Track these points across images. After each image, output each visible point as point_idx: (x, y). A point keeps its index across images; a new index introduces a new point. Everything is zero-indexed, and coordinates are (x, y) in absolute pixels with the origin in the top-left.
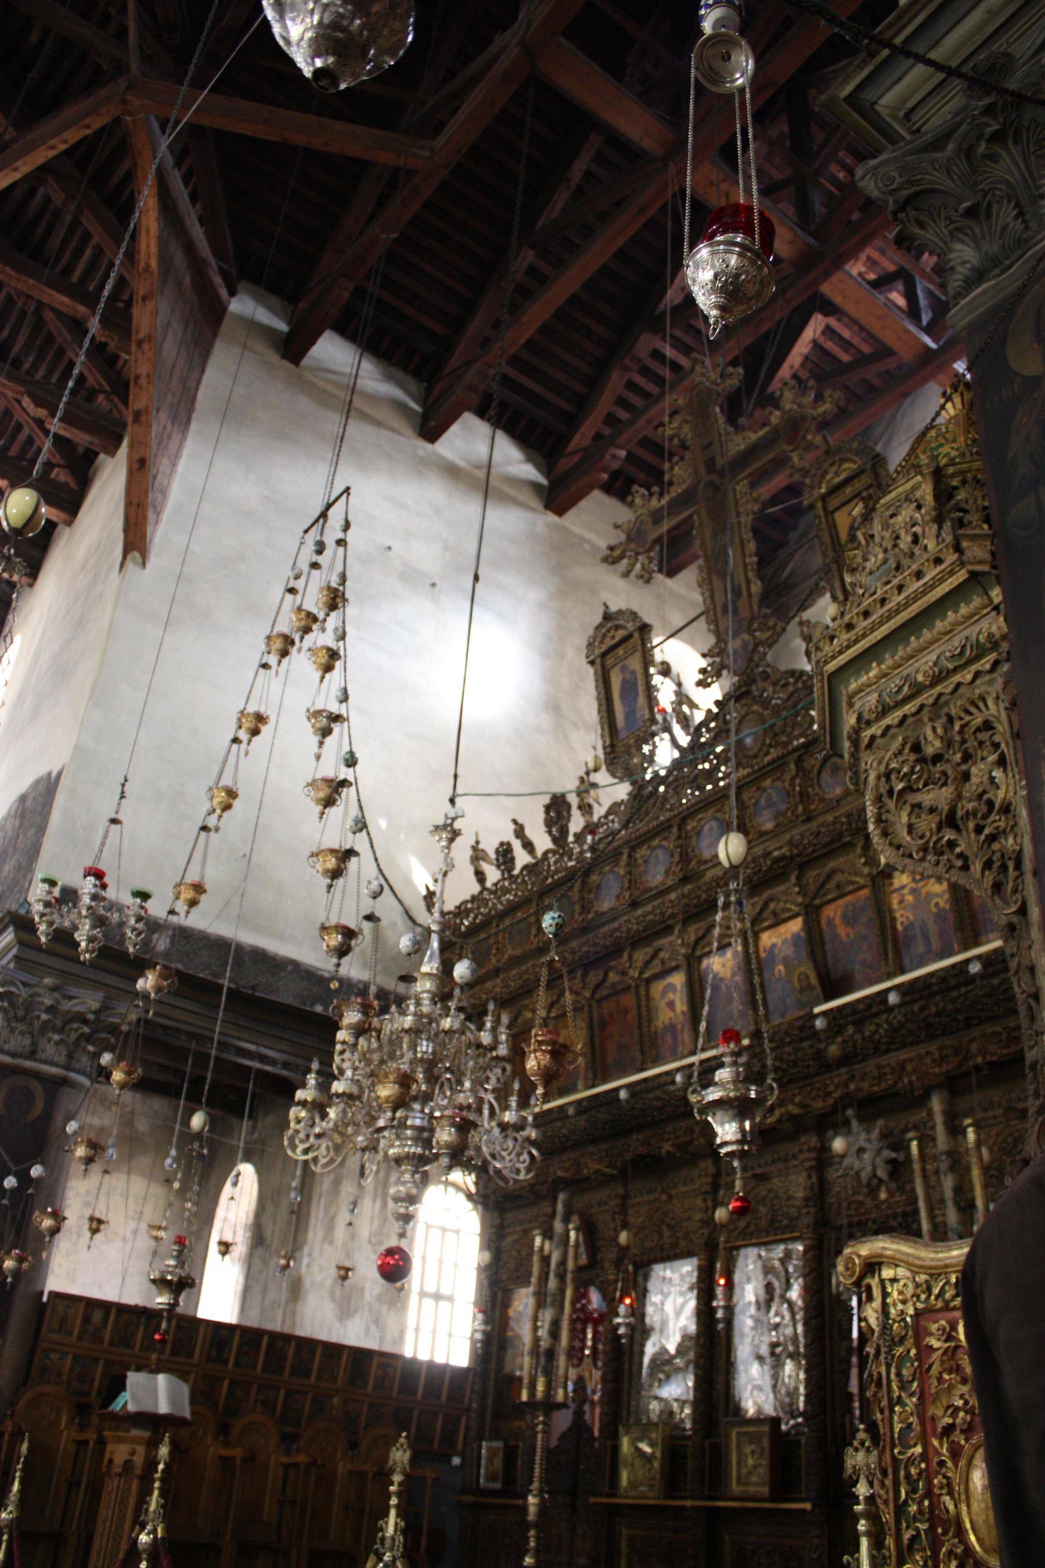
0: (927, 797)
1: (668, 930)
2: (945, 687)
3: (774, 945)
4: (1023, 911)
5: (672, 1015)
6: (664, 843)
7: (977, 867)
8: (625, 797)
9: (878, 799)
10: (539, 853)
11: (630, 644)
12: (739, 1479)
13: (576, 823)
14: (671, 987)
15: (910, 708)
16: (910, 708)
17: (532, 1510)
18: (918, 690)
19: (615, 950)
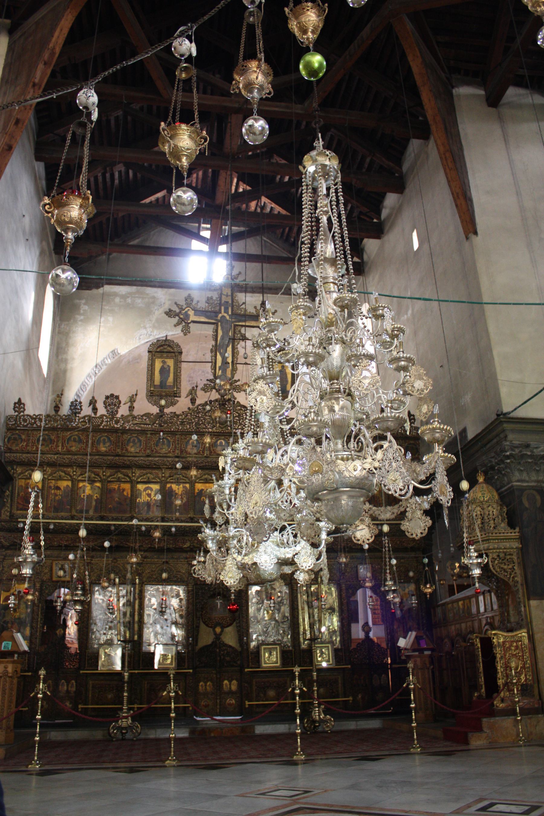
0: (502, 566)
1: (159, 468)
2: (508, 550)
3: (202, 490)
4: (518, 589)
5: (149, 499)
6: (169, 438)
7: (511, 579)
8: (155, 413)
9: (492, 562)
10: (99, 414)
11: (170, 355)
13: (123, 411)
14: (151, 489)
15: (501, 550)
16: (501, 550)
17: (126, 677)
18: (505, 548)
19: (129, 467)
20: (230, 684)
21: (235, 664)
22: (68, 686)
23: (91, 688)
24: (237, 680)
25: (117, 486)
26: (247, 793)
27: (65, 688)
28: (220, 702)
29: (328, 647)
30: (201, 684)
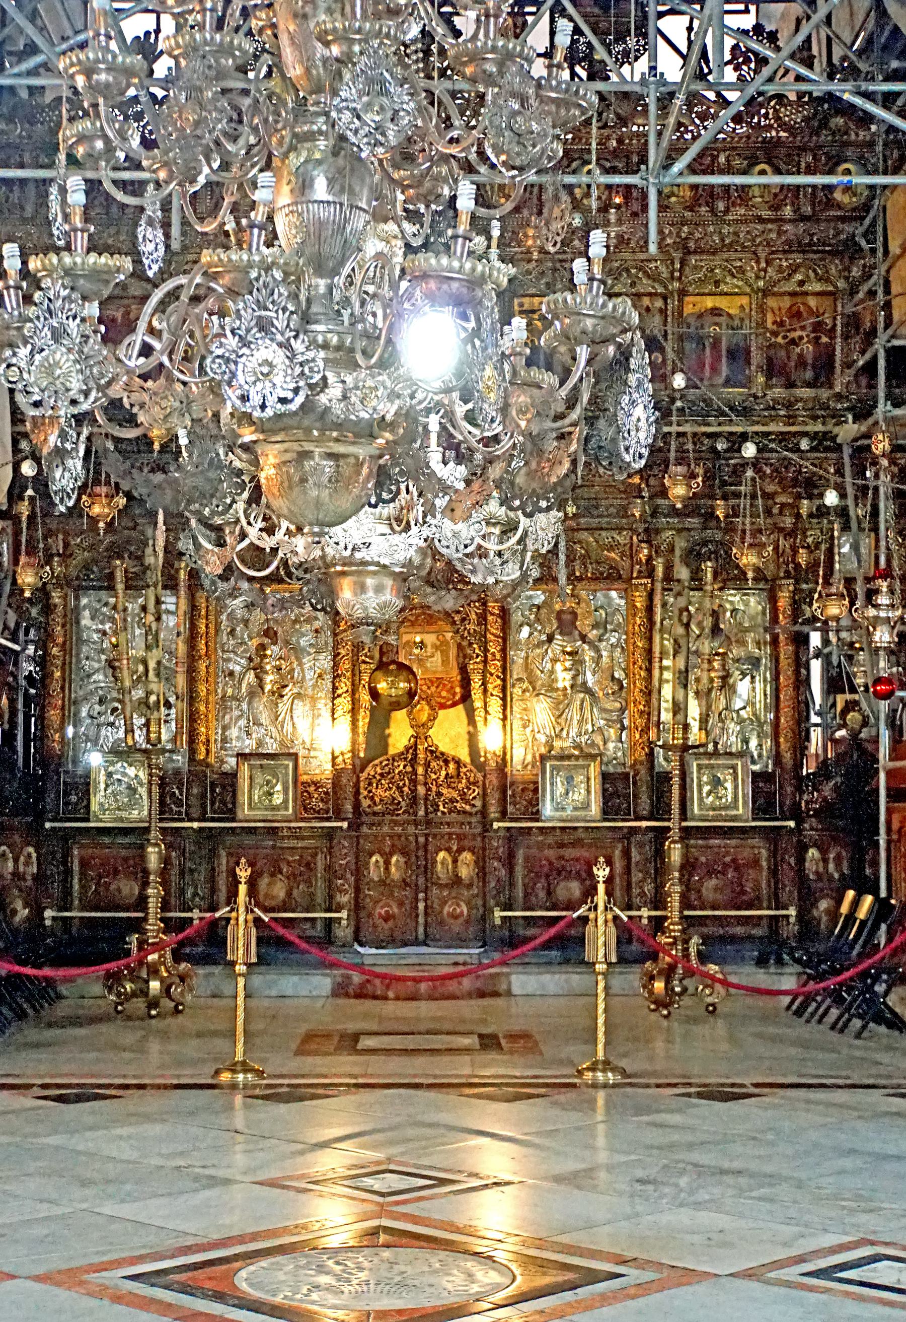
12: (250, 804)
20: (455, 861)
21: (468, 808)
22: (16, 860)
23: (76, 867)
24: (472, 850)
25: (122, 310)
26: (290, 1178)
27: (10, 864)
28: (426, 907)
29: (734, 768)
30: (374, 859)
